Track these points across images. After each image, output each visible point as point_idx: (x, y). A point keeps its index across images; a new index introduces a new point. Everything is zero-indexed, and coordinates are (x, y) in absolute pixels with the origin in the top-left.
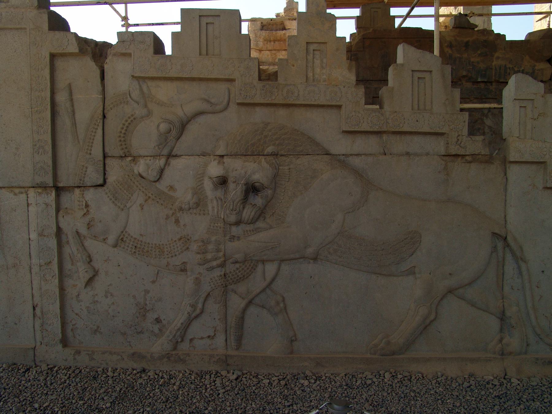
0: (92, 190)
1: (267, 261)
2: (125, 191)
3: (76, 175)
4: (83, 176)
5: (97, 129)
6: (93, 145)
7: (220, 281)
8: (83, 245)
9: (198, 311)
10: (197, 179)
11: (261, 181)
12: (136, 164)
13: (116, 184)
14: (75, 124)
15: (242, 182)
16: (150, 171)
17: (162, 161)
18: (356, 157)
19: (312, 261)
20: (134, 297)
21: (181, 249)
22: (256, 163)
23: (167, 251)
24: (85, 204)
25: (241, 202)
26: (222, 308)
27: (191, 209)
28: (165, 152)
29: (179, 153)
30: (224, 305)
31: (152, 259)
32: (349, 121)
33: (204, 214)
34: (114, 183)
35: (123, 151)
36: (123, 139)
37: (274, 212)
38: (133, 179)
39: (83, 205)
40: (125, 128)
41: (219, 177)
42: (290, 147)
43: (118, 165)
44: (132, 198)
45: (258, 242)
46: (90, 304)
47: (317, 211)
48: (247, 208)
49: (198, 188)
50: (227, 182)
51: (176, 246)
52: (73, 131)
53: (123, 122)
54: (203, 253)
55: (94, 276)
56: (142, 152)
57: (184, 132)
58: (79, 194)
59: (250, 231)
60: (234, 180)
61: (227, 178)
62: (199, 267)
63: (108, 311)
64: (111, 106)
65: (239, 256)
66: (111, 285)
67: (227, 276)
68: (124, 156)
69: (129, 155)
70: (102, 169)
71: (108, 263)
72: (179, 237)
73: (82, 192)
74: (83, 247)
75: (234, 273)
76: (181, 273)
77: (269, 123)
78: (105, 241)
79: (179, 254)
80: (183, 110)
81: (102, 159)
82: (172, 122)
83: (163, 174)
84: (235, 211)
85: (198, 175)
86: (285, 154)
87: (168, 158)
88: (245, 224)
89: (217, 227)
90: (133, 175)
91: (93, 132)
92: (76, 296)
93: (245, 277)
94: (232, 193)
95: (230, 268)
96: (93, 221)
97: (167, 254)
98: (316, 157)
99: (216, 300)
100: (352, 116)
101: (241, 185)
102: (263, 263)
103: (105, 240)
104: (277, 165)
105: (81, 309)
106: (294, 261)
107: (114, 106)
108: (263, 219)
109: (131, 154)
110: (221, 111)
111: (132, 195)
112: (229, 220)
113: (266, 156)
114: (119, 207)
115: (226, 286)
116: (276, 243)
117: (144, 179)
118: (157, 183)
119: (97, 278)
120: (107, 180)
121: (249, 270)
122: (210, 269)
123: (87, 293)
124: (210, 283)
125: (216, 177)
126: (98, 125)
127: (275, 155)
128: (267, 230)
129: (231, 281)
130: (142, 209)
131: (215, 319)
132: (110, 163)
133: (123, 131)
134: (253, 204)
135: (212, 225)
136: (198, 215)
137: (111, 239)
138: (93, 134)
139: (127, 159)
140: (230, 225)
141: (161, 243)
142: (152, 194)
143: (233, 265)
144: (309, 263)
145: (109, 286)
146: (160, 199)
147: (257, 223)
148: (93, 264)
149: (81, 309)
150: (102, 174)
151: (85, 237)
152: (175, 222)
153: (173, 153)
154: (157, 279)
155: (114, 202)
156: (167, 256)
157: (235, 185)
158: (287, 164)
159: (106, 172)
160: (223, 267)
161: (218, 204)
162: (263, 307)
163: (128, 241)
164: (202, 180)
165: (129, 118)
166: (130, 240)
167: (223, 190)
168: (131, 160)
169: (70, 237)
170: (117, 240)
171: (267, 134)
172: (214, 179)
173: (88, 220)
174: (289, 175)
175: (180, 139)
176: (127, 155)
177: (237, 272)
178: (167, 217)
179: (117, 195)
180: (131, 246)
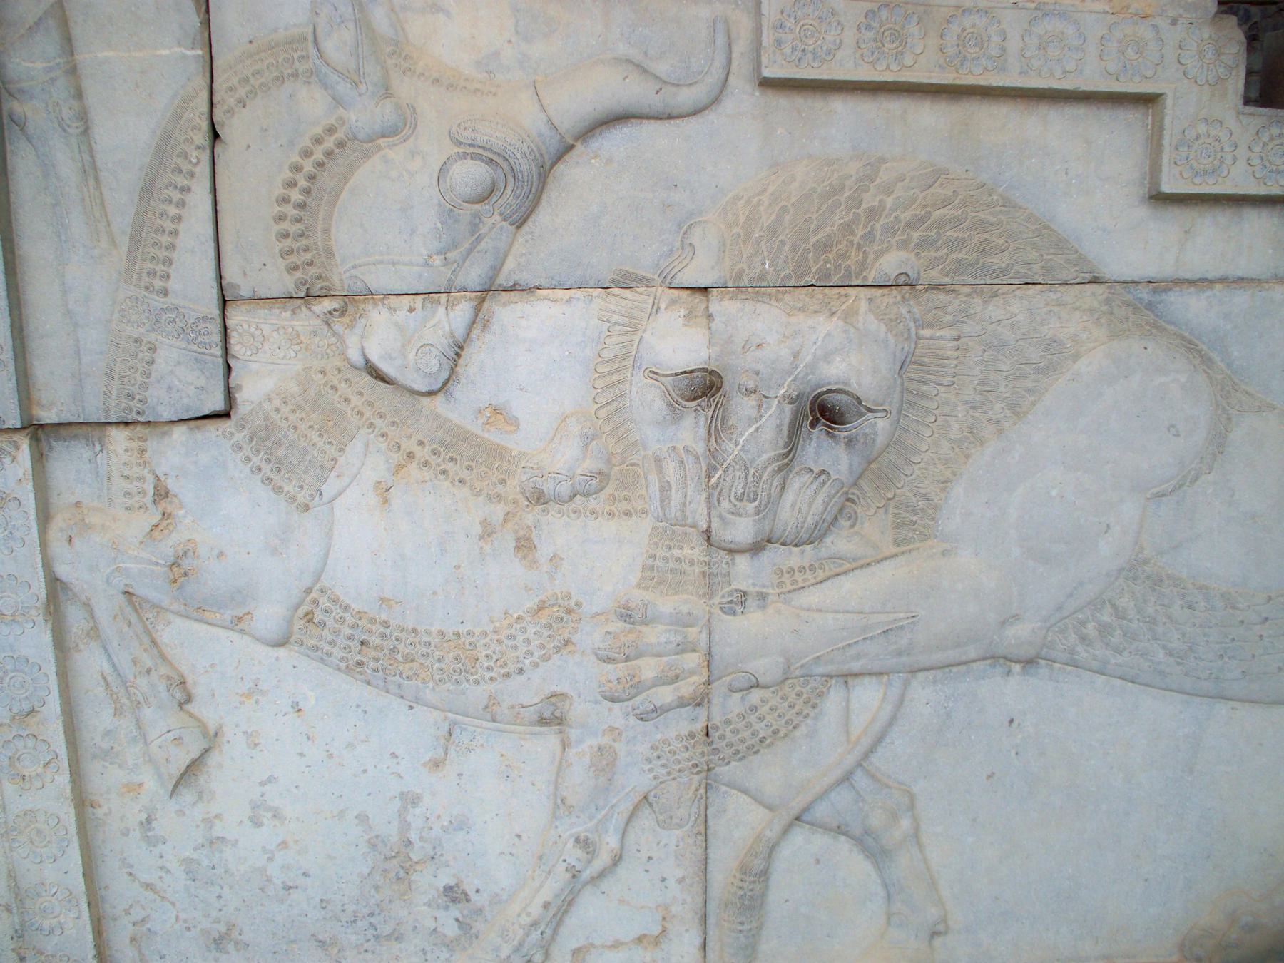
0: (179, 432)
1: (856, 675)
2: (316, 438)
3: (112, 379)
4: (140, 380)
5: (189, 190)
6: (175, 255)
7: (686, 755)
8: (154, 642)
9: (603, 859)
10: (598, 378)
11: (854, 387)
12: (351, 326)
13: (278, 410)
14: (95, 169)
15: (782, 392)
16: (411, 356)
17: (462, 310)
18: (1192, 289)
19: (1017, 668)
20: (362, 818)
21: (542, 647)
22: (835, 319)
23: (487, 656)
24: (155, 488)
25: (776, 465)
26: (691, 841)
27: (578, 497)
28: (474, 275)
29: (525, 278)
30: (699, 833)
31: (431, 684)
32: (1184, 155)
33: (627, 514)
34: (266, 406)
35: (298, 274)
36: (295, 228)
37: (890, 495)
38: (343, 385)
39: (143, 493)
40: (303, 183)
41: (692, 371)
42: (961, 256)
43: (282, 332)
44: (342, 460)
45: (837, 612)
46: (195, 849)
47: (1054, 493)
48: (796, 486)
49: (603, 413)
50: (719, 389)
51: (521, 637)
52: (87, 199)
53: (296, 158)
54: (627, 659)
55: (207, 751)
56: (379, 280)
57: (544, 197)
58: (127, 450)
59: (802, 569)
60: (751, 385)
61: (720, 377)
62: (610, 710)
63: (266, 871)
64: (242, 92)
65: (765, 667)
66: (271, 780)
67: (715, 735)
68: (302, 294)
69: (323, 292)
70: (218, 351)
71: (257, 702)
72: (531, 603)
73: (136, 445)
74: (155, 651)
75: (741, 725)
76: (538, 729)
77: (882, 160)
78: (240, 626)
79: (536, 665)
80: (543, 109)
81: (216, 312)
82: (499, 154)
83: (461, 362)
84: (754, 500)
85: (604, 362)
86: (946, 280)
87: (483, 300)
88: (783, 544)
89: (678, 560)
90: (339, 370)
91: (171, 202)
92: (141, 823)
93: (781, 734)
94: (742, 435)
95: (727, 707)
96: (190, 553)
97: (488, 669)
98: (1059, 295)
99: (671, 818)
100: (1197, 138)
101: (776, 402)
102: (846, 682)
103: (240, 619)
104: (912, 325)
105: (162, 868)
106: (955, 669)
107: (252, 93)
108: (848, 523)
109: (329, 289)
110: (696, 112)
111: (341, 450)
112: (730, 538)
113: (874, 290)
114: (294, 499)
115: (709, 769)
116: (901, 615)
117: (387, 383)
118: (440, 398)
119: (213, 759)
120: (237, 395)
121: (795, 711)
122: (654, 715)
123: (181, 813)
124: (649, 760)
125: (676, 375)
126: (192, 175)
127: (907, 284)
128: (868, 564)
129: (728, 752)
130: (386, 501)
131: (663, 880)
132: (246, 326)
133: (296, 196)
134: (816, 470)
135: (661, 553)
136: (607, 517)
137: (269, 615)
138: (172, 211)
139: (314, 308)
140: (731, 551)
141: (462, 630)
142: (421, 443)
143: (739, 695)
144: (1009, 673)
145: (262, 784)
146: (452, 459)
147: (828, 540)
148: (202, 708)
149: (162, 868)
150: (221, 371)
151: (158, 608)
152: (518, 548)
153: (502, 280)
154: (446, 754)
155: (271, 480)
156: (488, 675)
157: (754, 403)
158: (950, 318)
159: (232, 362)
160: (699, 705)
161: (684, 477)
162: (840, 830)
163: (330, 622)
164: (621, 382)
165: (318, 141)
166: (342, 620)
167: (703, 419)
168: (330, 313)
169: (103, 615)
170: (290, 622)
171: (876, 203)
172: (670, 378)
173: (171, 552)
174: (955, 362)
175: (530, 222)
176: (315, 291)
177: (753, 718)
178: (488, 531)
179: (281, 452)
180: (348, 643)
